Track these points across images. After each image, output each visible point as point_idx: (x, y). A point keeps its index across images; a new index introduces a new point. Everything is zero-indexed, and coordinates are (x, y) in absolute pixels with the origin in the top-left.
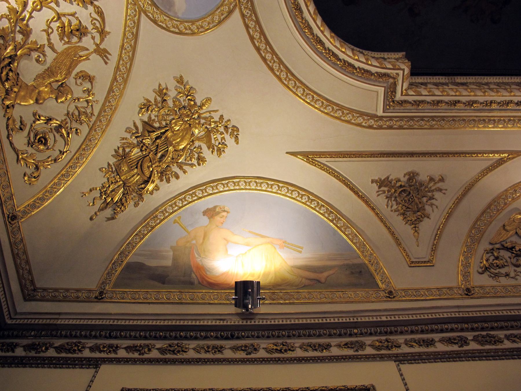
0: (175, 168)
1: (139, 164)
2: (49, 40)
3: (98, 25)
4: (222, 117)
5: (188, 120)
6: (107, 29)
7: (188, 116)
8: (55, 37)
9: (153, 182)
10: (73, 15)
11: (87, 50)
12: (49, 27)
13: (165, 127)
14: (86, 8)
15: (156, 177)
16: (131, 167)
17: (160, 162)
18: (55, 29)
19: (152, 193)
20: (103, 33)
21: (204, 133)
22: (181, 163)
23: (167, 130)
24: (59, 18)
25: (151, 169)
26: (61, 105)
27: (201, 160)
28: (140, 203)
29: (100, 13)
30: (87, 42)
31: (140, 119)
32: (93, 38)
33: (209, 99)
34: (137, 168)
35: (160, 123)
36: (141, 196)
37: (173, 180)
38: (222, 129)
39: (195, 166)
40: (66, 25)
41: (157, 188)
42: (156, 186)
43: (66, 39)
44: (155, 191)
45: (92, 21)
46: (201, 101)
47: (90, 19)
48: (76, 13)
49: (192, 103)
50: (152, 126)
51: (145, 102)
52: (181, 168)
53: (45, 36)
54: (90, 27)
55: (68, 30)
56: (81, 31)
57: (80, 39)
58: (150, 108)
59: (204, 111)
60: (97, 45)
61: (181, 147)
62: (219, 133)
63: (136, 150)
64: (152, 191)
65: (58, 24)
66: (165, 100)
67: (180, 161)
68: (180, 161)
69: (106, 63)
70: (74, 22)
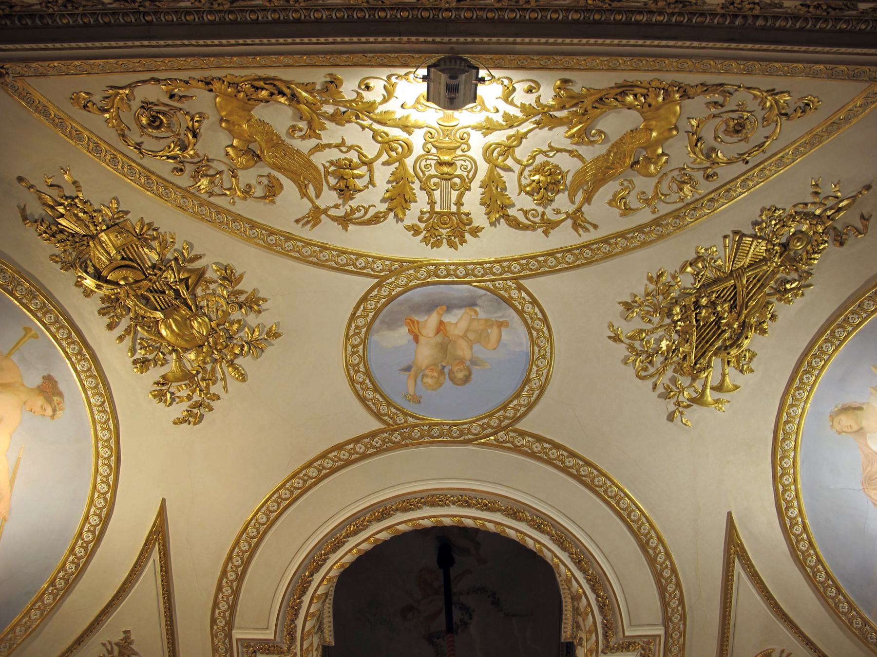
0: (125, 323)
1: (128, 262)
2: (329, 146)
3: (357, 215)
5: (209, 343)
6: (351, 227)
7: (216, 343)
8: (334, 154)
9: (99, 287)
10: (371, 182)
12: (350, 148)
13: (197, 306)
14: (383, 200)
15: (106, 290)
16: (123, 249)
17: (136, 296)
18: (348, 156)
19: (79, 284)
20: (345, 221)
21: (190, 368)
22: (136, 332)
23: (191, 310)
24: (364, 163)
25: (122, 283)
26: (223, 153)
27: (143, 364)
28: (59, 265)
29: (376, 219)
30: (329, 198)
31: (208, 266)
32: (336, 206)
33: (243, 378)
34: (123, 258)
35: (203, 298)
36: (72, 266)
37: (106, 320)
39: (133, 355)
40: (356, 172)
41: (88, 293)
42: (92, 291)
43: (332, 169)
44: (82, 290)
45: (363, 207)
46: (240, 366)
47: (366, 206)
48: (374, 186)
49: (237, 352)
50: (196, 284)
51: (237, 275)
52: (128, 331)
53: (334, 142)
54: (353, 203)
55: (347, 174)
56: (346, 191)
58: (226, 283)
59: (225, 370)
61: (164, 332)
62: (192, 395)
63: (155, 257)
64: (81, 285)
65: (355, 160)
66: (241, 308)
67: (139, 328)
68: (139, 328)
70: (360, 183)
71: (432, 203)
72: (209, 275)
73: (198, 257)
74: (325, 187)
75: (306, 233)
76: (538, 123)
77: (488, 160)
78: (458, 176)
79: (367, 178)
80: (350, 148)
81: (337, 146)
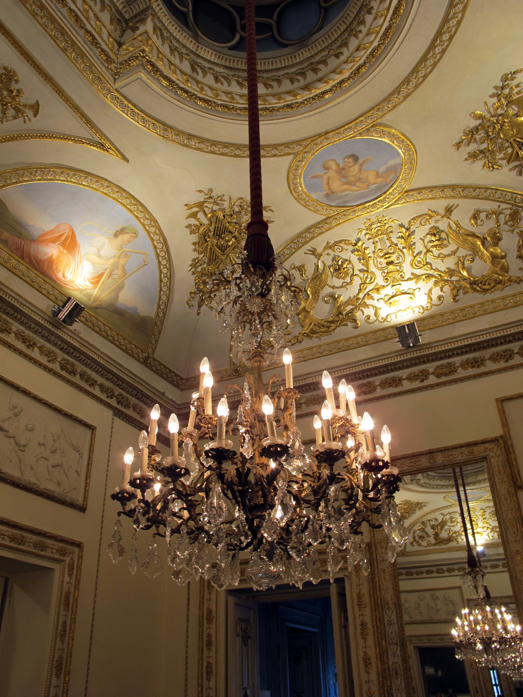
2: (449, 255)
4: (492, 96)
8: (446, 251)
11: (449, 223)
30: (442, 225)
32: (437, 221)
35: (508, 147)
38: (506, 91)
56: (435, 232)
57: (442, 231)
60: (442, 217)
69: (458, 206)
71: (389, 239)
72: (504, 162)
73: (510, 170)
74: (446, 231)
75: (451, 202)
76: (358, 299)
77: (372, 273)
78: (382, 257)
79: (426, 241)
80: (438, 257)
81: (445, 256)
